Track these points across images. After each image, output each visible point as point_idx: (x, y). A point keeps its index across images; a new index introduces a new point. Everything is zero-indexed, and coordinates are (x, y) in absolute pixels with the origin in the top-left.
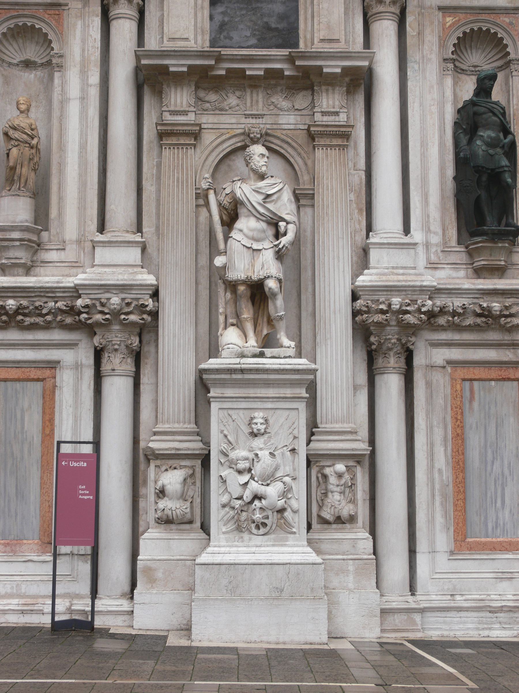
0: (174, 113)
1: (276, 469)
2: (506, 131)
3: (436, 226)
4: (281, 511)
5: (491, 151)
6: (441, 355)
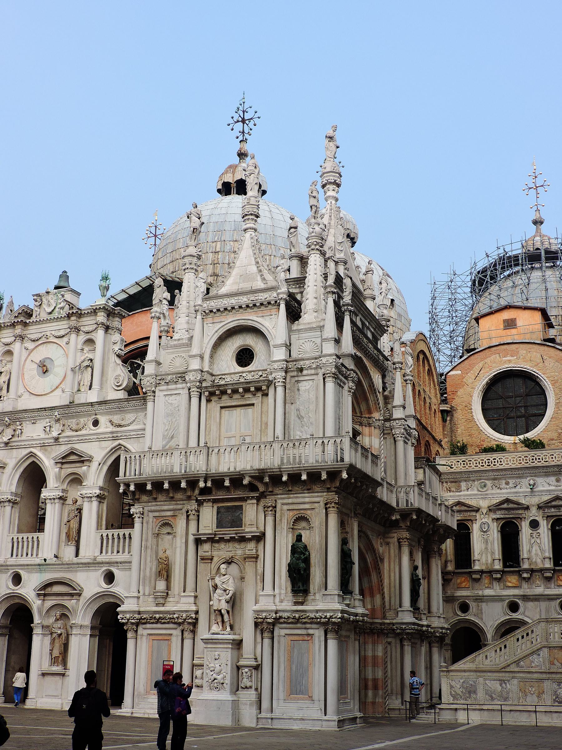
0: (205, 552)
1: (221, 670)
3: (284, 587)
4: (223, 684)
6: (283, 632)
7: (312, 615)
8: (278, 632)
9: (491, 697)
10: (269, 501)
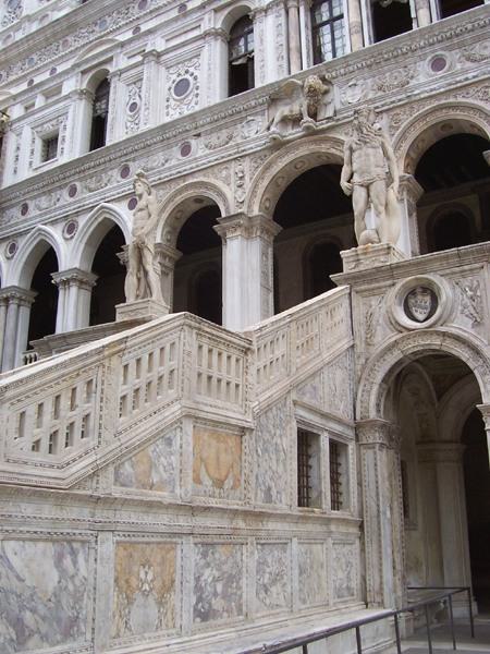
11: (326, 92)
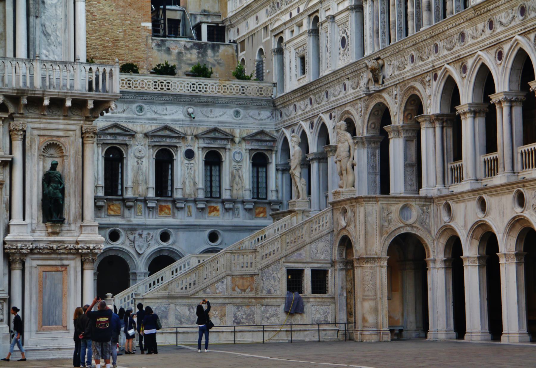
2: (61, 184)
3: (35, 217)
5: (55, 191)
6: (35, 263)
7: (71, 246)
8: (31, 263)
9: (180, 321)
10: (18, 123)
11: (383, 66)
